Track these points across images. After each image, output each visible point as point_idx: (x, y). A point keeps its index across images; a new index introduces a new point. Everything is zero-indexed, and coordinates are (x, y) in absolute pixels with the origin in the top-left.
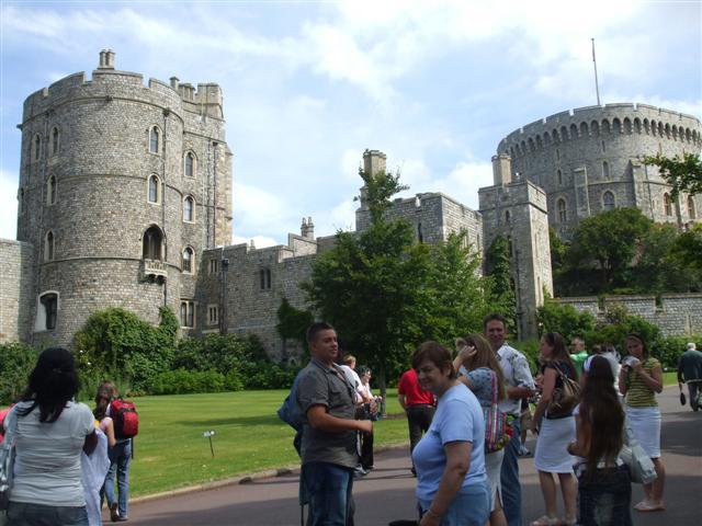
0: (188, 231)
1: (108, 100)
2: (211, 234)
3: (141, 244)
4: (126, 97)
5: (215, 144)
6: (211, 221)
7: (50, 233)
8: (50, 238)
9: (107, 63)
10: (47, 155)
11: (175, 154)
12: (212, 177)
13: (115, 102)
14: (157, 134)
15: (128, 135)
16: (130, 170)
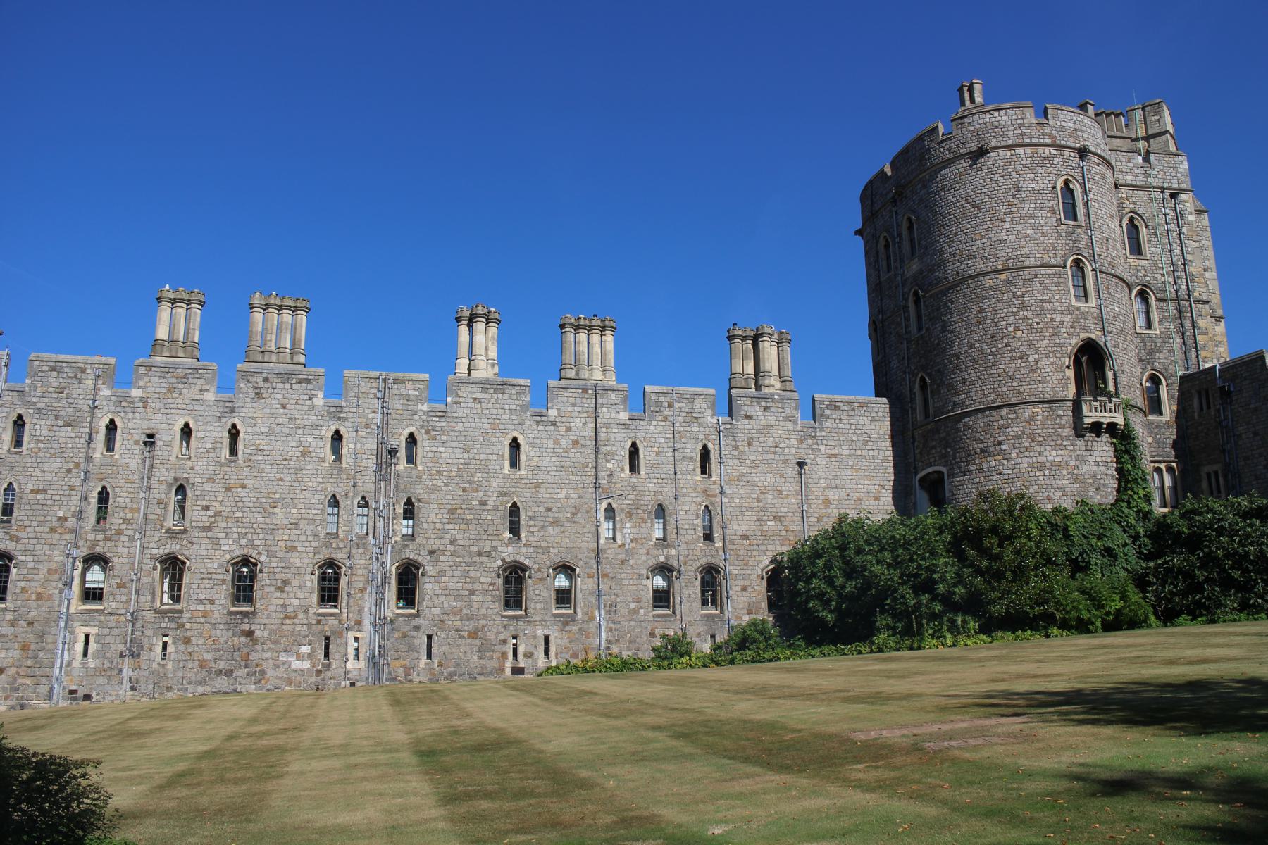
0: (1148, 350)
1: (982, 152)
2: (1190, 344)
3: (1070, 373)
4: (1010, 142)
5: (1174, 196)
6: (1188, 325)
7: (923, 379)
8: (923, 386)
9: (972, 100)
10: (902, 261)
11: (1110, 227)
12: (1177, 251)
13: (993, 154)
14: (1072, 192)
15: (1023, 202)
16: (1035, 254)
